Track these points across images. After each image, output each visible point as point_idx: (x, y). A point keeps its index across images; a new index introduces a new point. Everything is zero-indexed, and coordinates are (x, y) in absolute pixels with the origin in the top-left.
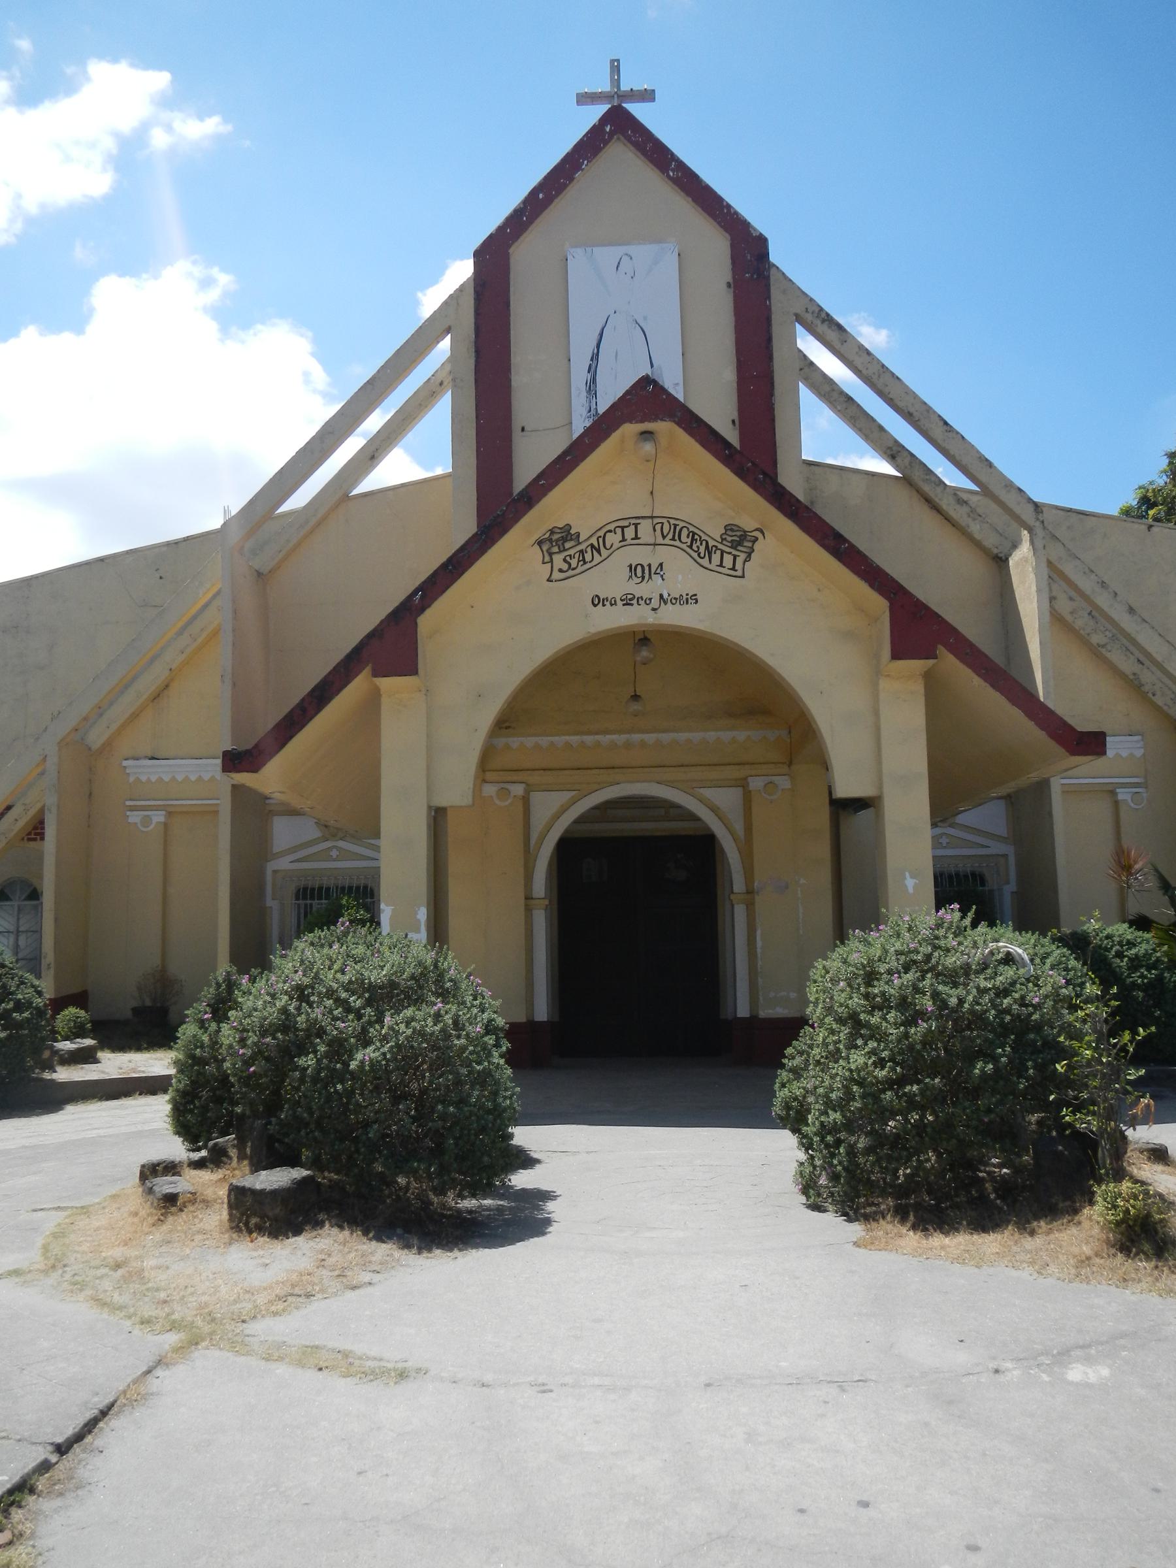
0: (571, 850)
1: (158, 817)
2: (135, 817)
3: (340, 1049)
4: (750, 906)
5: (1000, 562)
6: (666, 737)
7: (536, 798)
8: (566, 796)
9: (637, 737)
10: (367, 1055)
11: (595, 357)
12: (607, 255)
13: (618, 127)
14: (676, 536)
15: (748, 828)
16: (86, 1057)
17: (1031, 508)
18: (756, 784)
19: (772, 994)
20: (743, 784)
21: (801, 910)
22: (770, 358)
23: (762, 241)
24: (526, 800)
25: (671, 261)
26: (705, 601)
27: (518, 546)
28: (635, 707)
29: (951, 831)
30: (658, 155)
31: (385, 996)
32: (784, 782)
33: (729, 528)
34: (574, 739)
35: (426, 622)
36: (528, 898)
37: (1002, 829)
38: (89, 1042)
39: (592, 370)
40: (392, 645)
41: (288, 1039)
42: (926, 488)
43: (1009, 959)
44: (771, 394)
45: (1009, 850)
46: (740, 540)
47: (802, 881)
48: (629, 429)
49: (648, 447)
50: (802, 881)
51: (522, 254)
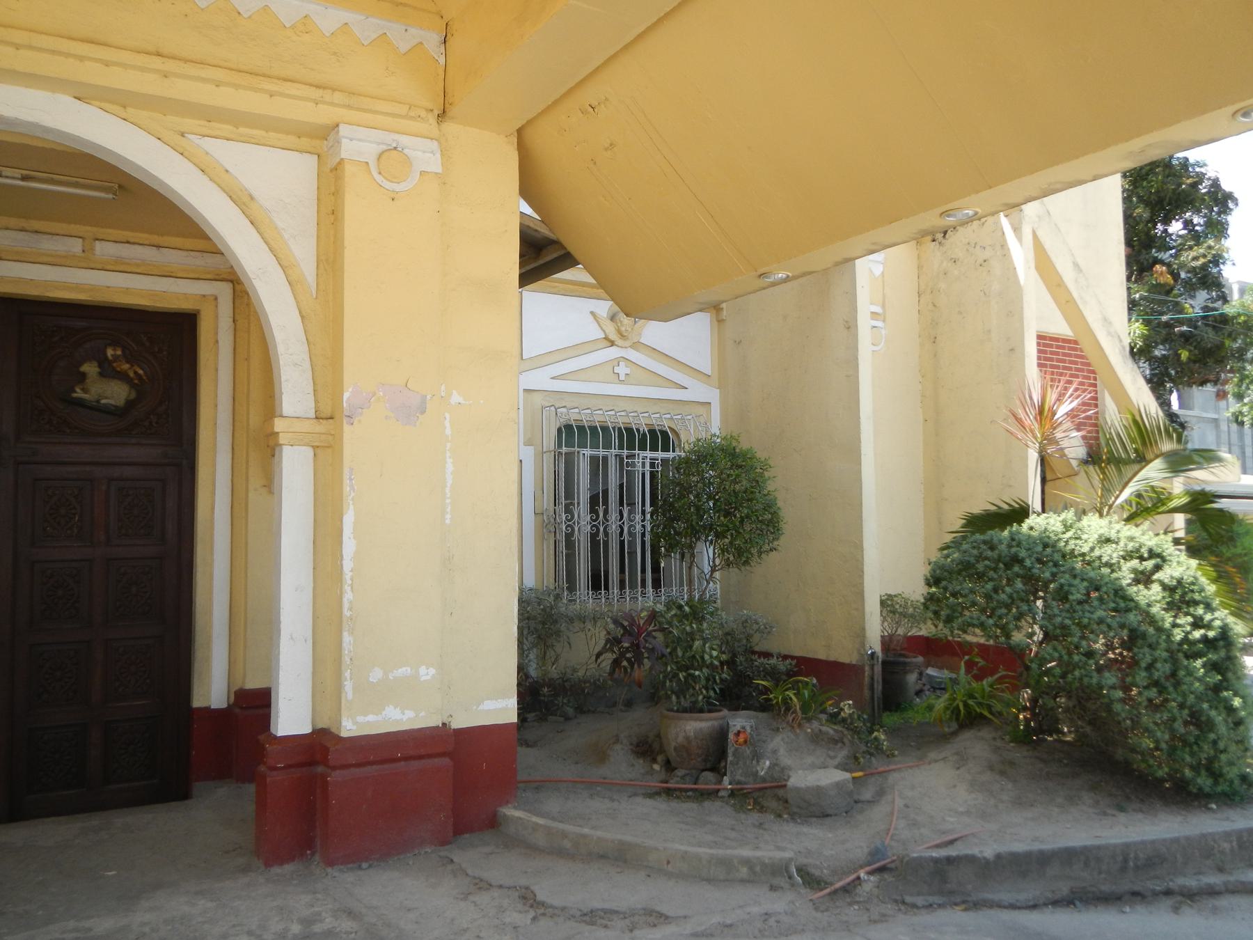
4: (327, 452)
18: (358, 144)
19: (376, 675)
20: (319, 139)
21: (450, 467)
29: (633, 355)
32: (424, 154)
37: (704, 362)
45: (712, 395)
47: (456, 398)
50: (456, 398)
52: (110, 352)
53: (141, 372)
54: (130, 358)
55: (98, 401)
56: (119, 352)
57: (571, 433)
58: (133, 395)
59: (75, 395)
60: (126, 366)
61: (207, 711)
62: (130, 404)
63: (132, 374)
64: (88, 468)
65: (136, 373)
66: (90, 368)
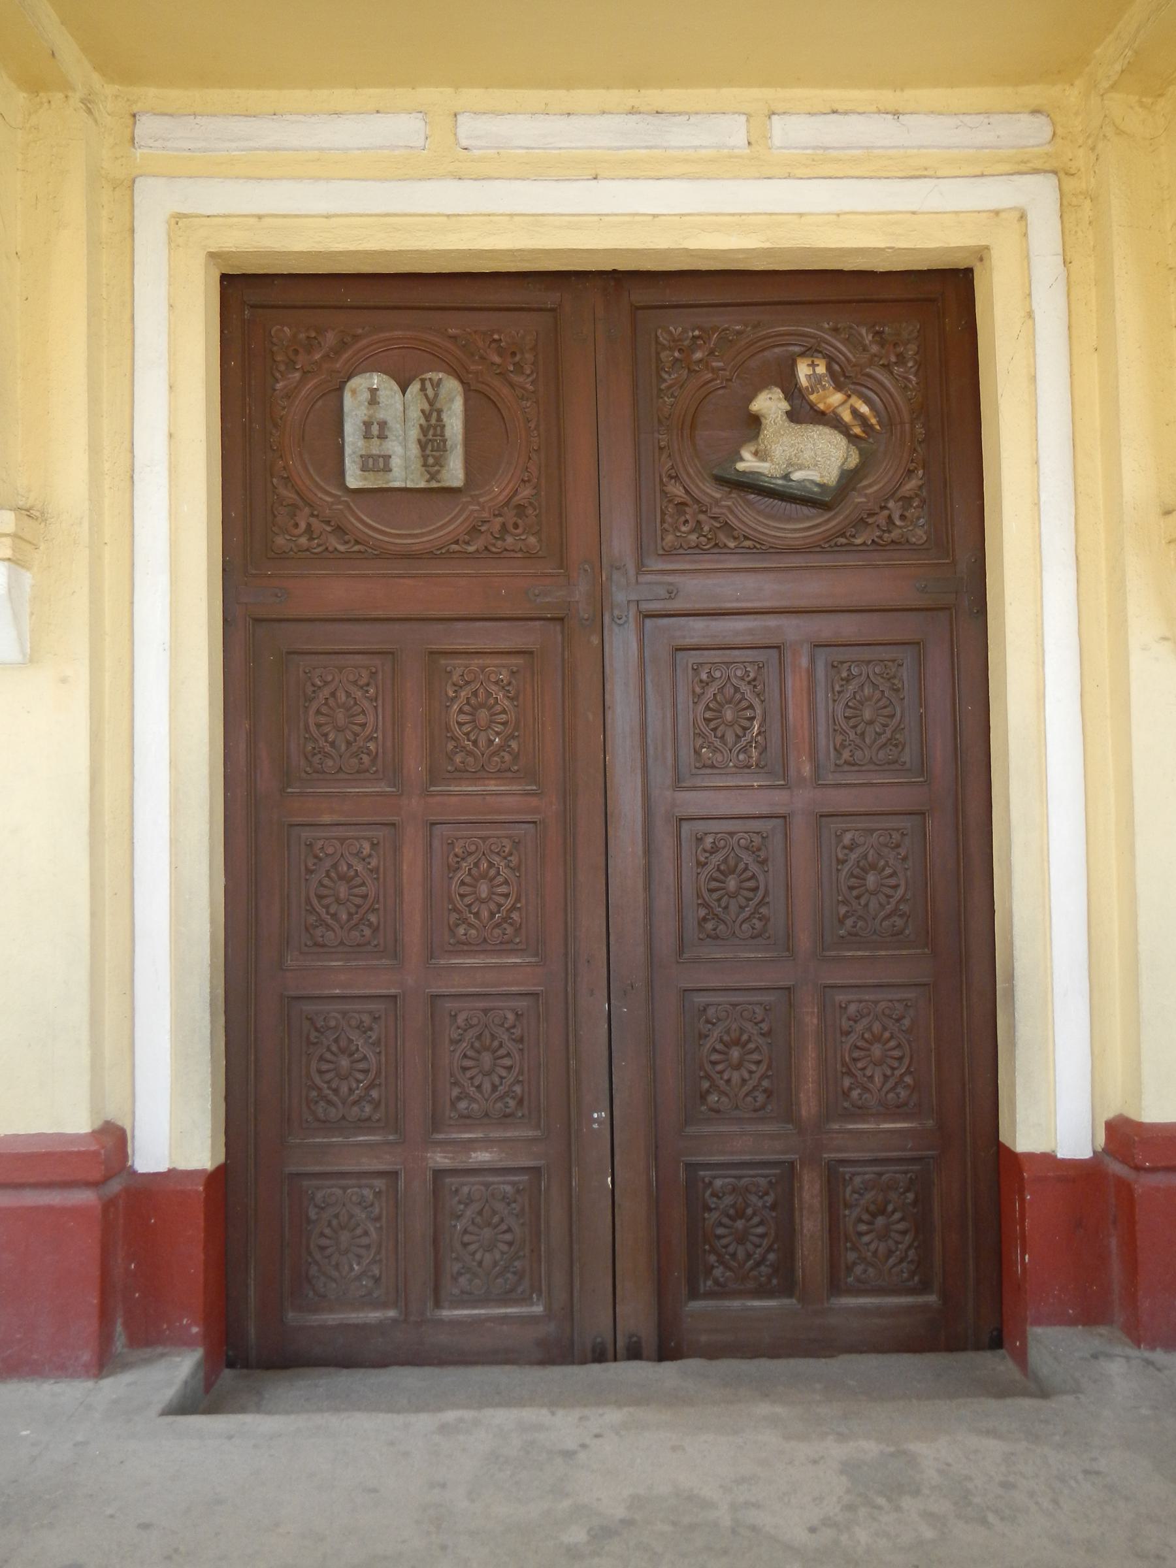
52: (803, 371)
53: (864, 409)
54: (840, 379)
55: (786, 477)
56: (821, 369)
58: (854, 461)
59: (741, 466)
60: (836, 398)
61: (1048, 1159)
62: (849, 479)
63: (847, 416)
64: (772, 622)
65: (855, 412)
66: (770, 404)
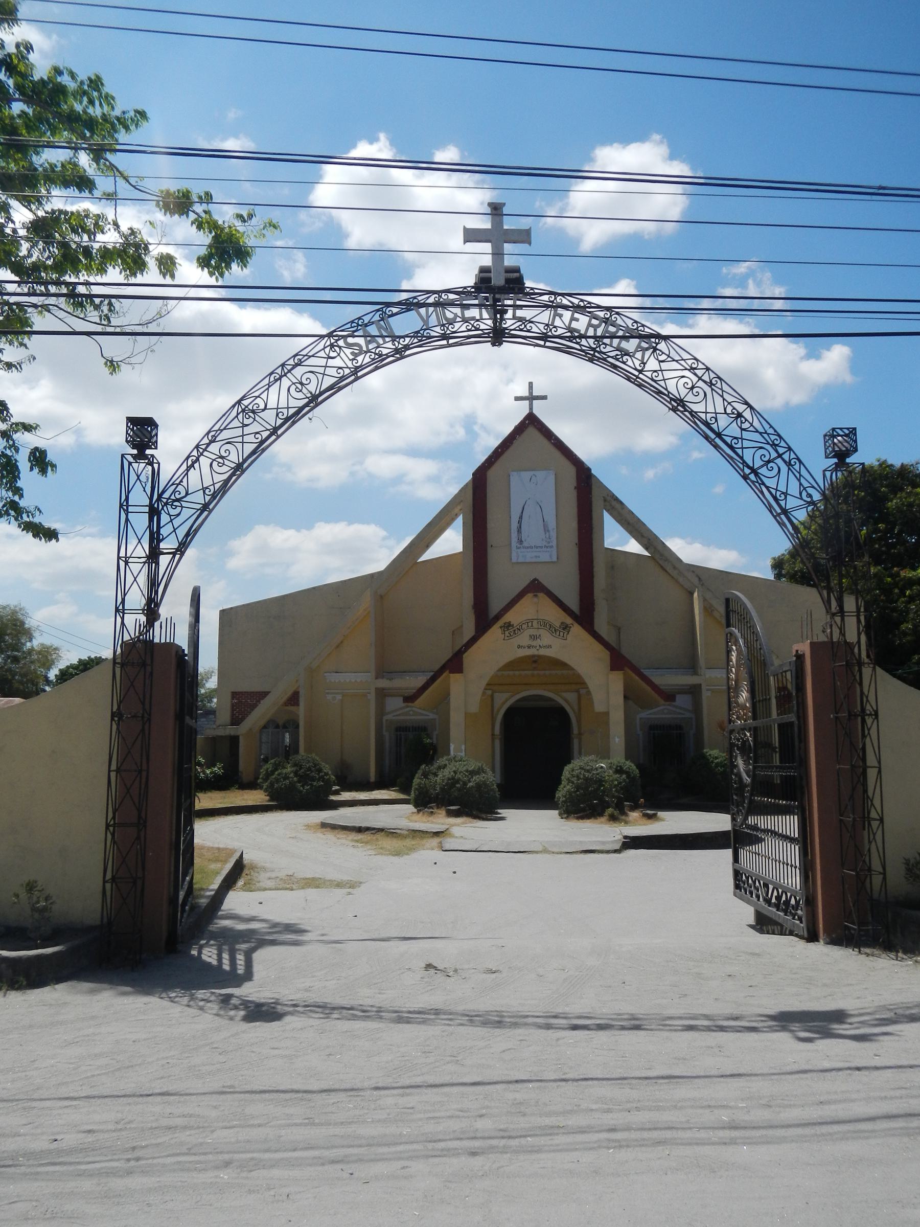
0: (510, 713)
1: (339, 697)
2: (329, 697)
3: (465, 784)
5: (692, 594)
6: (547, 672)
7: (496, 695)
8: (510, 694)
9: (536, 672)
10: (471, 784)
11: (521, 517)
12: (526, 475)
13: (531, 421)
14: (545, 625)
15: (580, 709)
16: (337, 793)
17: (697, 579)
20: (578, 691)
22: (591, 519)
23: (589, 470)
24: (492, 697)
25: (552, 478)
26: (552, 646)
27: (495, 633)
28: (534, 665)
30: (548, 434)
31: (473, 773)
33: (562, 623)
34: (511, 673)
35: (468, 657)
36: (493, 735)
38: (337, 787)
39: (520, 522)
40: (455, 664)
41: (453, 782)
42: (661, 562)
43: (602, 767)
44: (591, 534)
46: (566, 627)
48: (530, 595)
49: (535, 600)
51: (491, 474)
57: (653, 727)
